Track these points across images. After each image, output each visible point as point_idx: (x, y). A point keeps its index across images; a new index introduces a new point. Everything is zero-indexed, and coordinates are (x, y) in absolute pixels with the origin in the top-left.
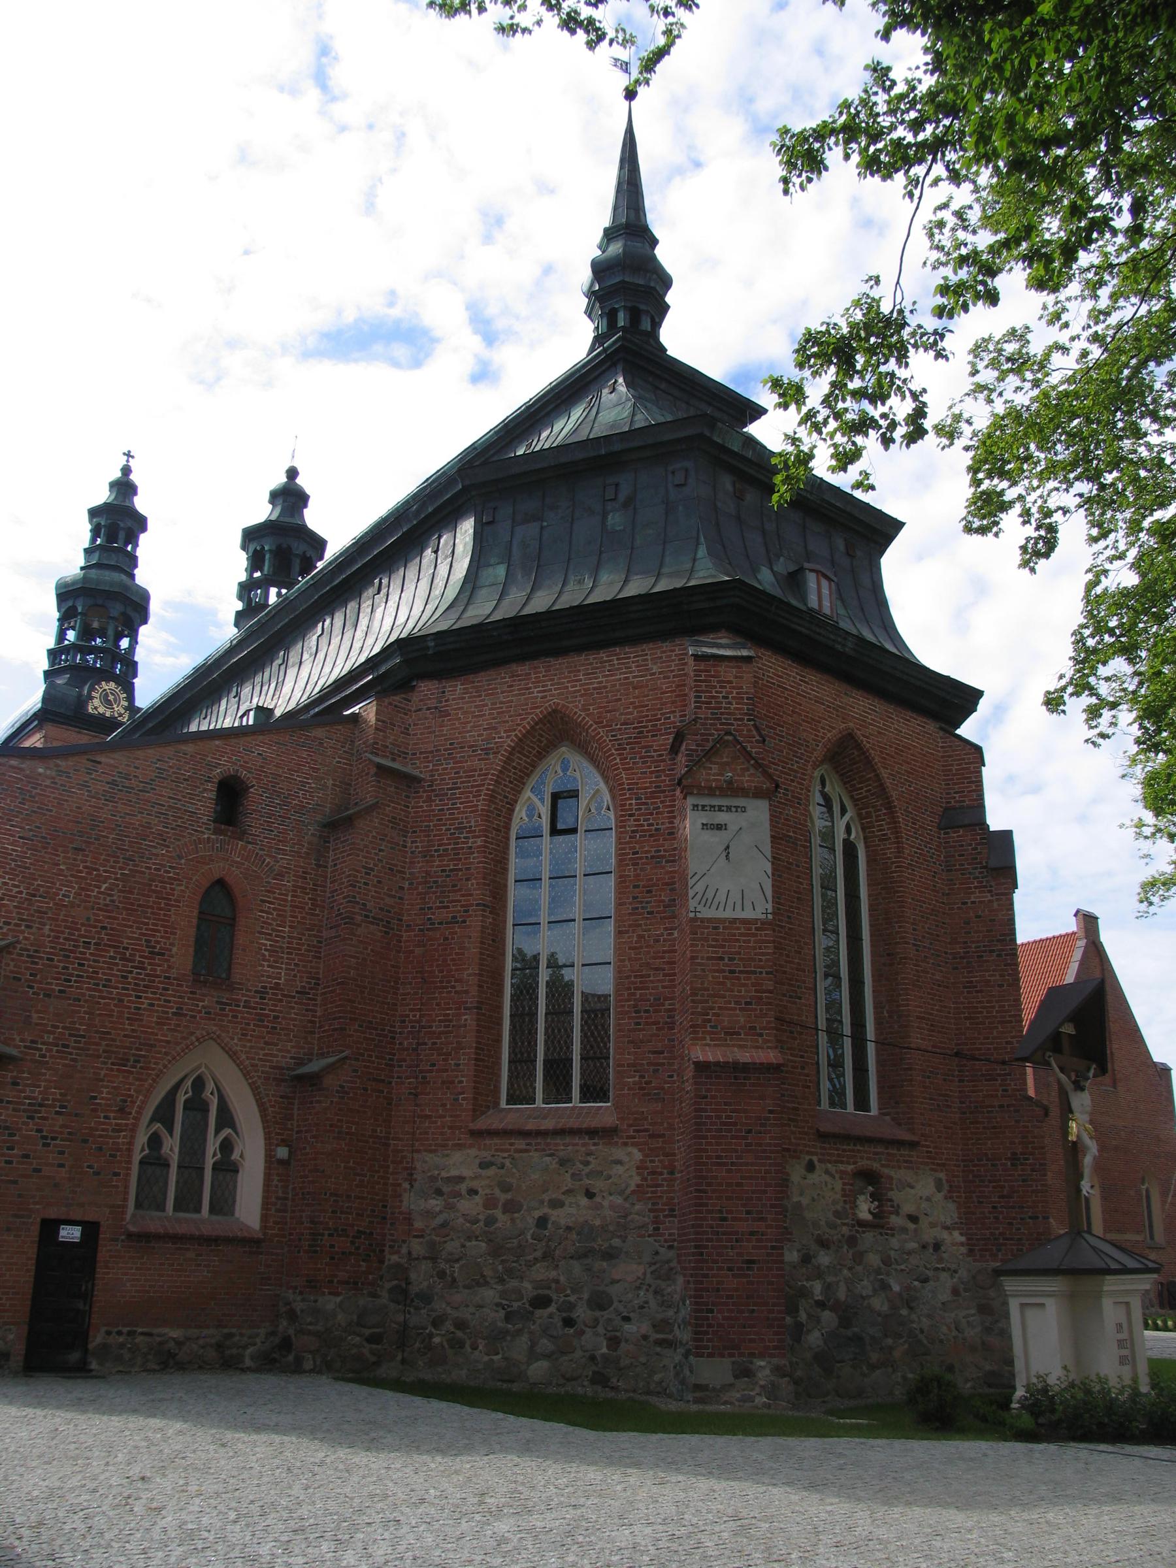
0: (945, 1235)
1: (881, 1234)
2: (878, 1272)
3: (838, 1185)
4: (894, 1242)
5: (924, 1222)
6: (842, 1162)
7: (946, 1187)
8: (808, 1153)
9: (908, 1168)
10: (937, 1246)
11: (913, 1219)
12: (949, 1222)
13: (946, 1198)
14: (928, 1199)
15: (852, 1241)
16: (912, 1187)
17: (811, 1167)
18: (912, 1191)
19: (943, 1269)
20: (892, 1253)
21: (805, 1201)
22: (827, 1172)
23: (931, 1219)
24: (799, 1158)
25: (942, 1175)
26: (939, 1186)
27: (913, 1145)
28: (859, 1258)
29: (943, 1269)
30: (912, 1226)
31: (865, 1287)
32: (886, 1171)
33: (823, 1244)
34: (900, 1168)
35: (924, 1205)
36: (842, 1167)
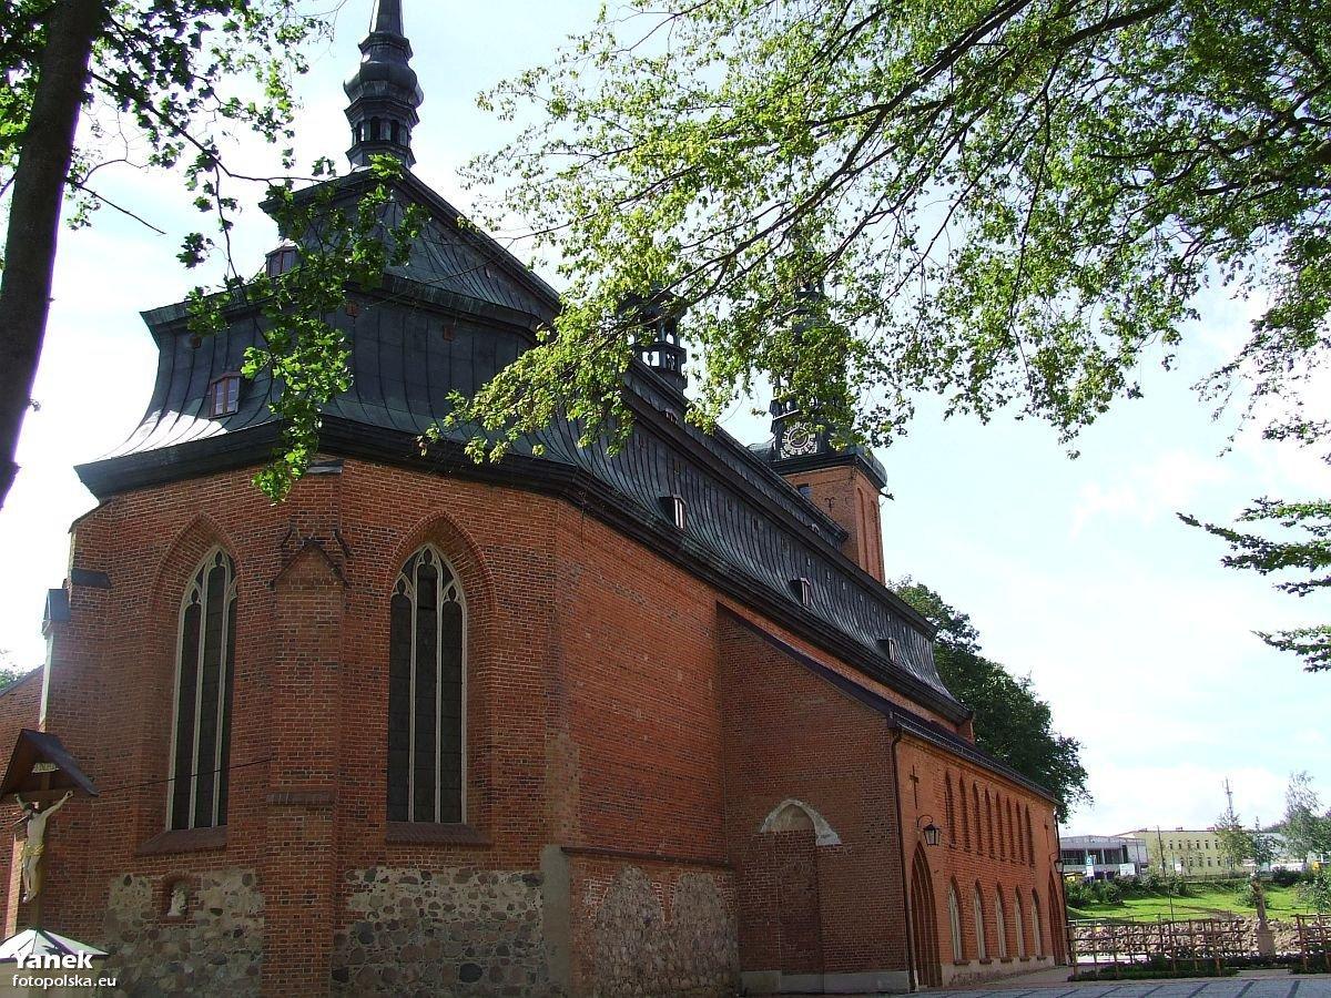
0: (250, 922)
1: (182, 927)
2: (175, 957)
3: (149, 892)
4: (193, 933)
5: (226, 916)
6: (154, 874)
7: (255, 880)
8: (126, 871)
9: (217, 869)
10: (239, 933)
11: (217, 911)
12: (254, 911)
13: (253, 890)
14: (234, 893)
15: (153, 935)
16: (218, 885)
17: (128, 881)
18: (219, 888)
19: (242, 952)
20: (191, 942)
21: (118, 908)
22: (141, 883)
23: (235, 911)
24: (118, 876)
25: (252, 871)
26: (247, 880)
27: (223, 849)
28: (159, 947)
29: (242, 952)
30: (214, 917)
31: (160, 970)
32: (195, 874)
33: (127, 938)
34: (209, 870)
35: (230, 898)
36: (153, 878)
